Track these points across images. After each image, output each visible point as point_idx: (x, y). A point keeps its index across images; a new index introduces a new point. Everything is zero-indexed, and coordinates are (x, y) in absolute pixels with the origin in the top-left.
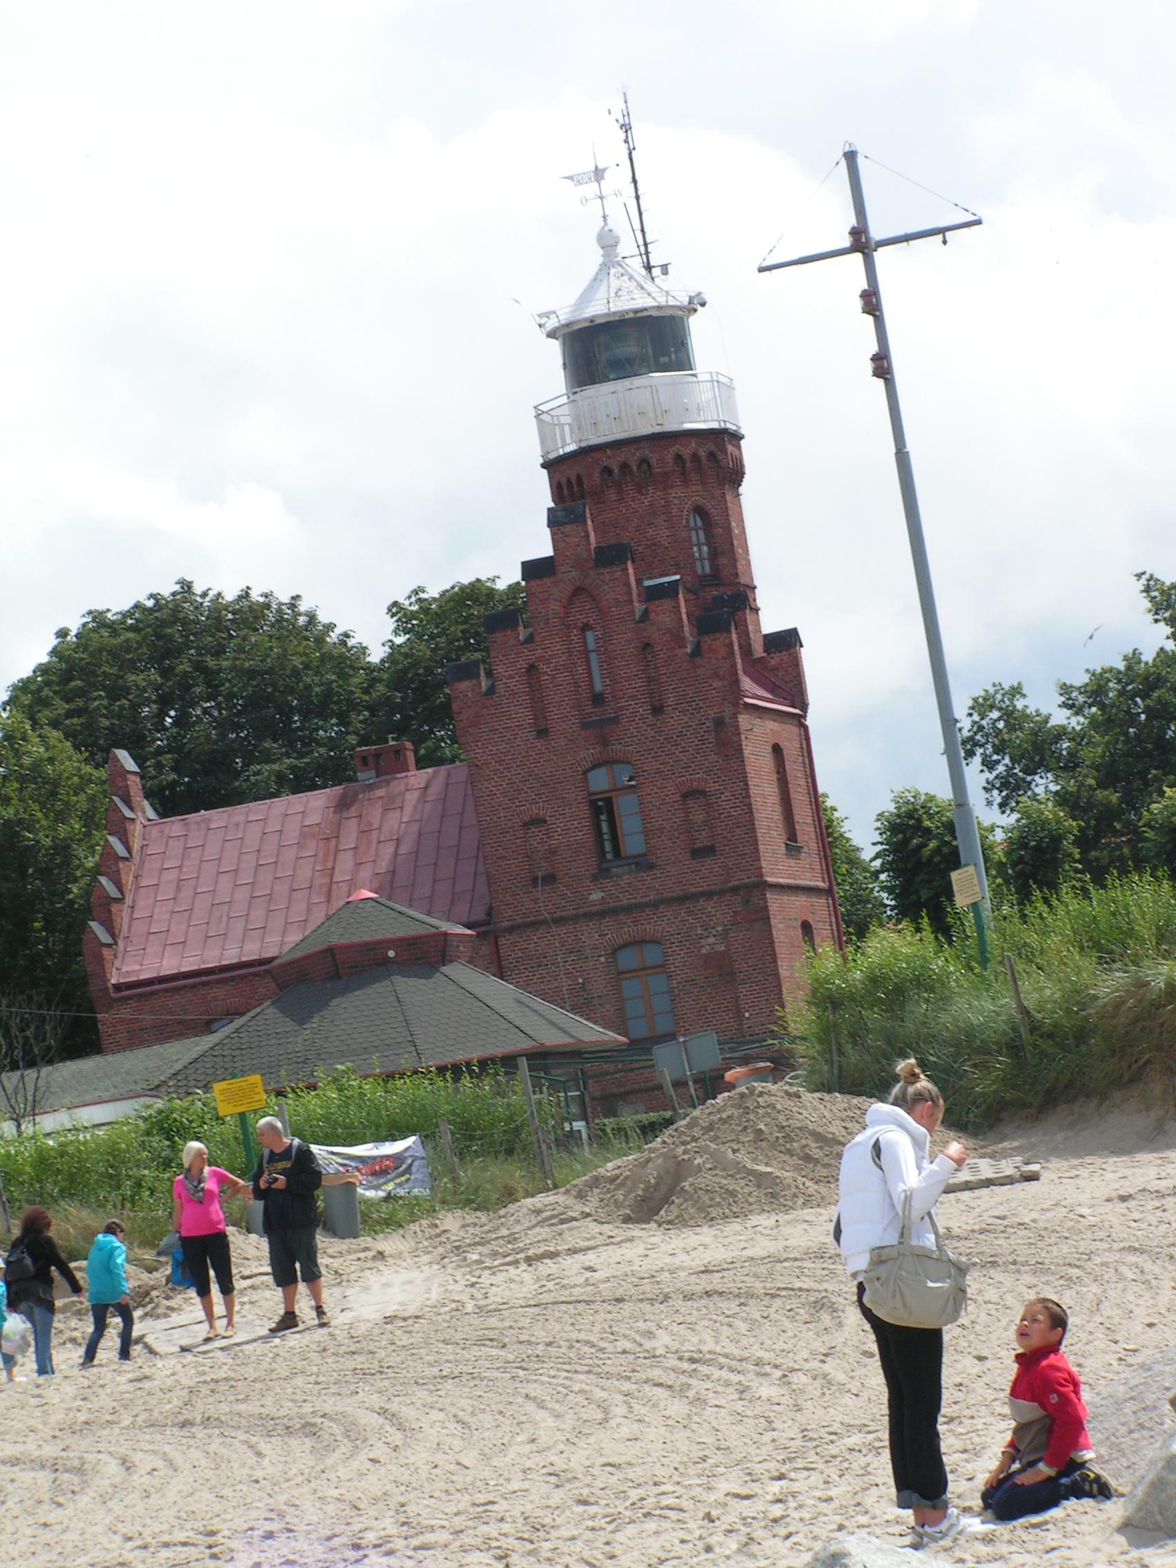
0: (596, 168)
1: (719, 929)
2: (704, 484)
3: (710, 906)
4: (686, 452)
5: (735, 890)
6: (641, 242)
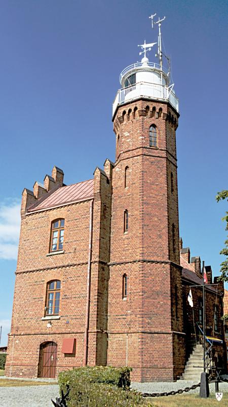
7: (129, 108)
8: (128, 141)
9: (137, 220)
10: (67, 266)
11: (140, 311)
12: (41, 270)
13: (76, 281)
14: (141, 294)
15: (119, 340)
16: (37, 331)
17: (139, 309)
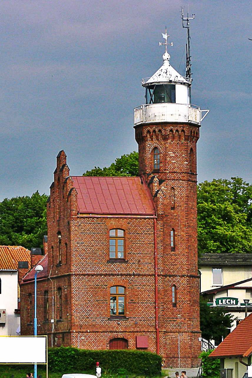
2: (158, 140)
7: (176, 128)
8: (174, 161)
9: (183, 240)
10: (133, 275)
11: (188, 316)
12: (103, 275)
13: (142, 290)
14: (189, 302)
15: (172, 338)
16: (104, 330)
17: (188, 314)
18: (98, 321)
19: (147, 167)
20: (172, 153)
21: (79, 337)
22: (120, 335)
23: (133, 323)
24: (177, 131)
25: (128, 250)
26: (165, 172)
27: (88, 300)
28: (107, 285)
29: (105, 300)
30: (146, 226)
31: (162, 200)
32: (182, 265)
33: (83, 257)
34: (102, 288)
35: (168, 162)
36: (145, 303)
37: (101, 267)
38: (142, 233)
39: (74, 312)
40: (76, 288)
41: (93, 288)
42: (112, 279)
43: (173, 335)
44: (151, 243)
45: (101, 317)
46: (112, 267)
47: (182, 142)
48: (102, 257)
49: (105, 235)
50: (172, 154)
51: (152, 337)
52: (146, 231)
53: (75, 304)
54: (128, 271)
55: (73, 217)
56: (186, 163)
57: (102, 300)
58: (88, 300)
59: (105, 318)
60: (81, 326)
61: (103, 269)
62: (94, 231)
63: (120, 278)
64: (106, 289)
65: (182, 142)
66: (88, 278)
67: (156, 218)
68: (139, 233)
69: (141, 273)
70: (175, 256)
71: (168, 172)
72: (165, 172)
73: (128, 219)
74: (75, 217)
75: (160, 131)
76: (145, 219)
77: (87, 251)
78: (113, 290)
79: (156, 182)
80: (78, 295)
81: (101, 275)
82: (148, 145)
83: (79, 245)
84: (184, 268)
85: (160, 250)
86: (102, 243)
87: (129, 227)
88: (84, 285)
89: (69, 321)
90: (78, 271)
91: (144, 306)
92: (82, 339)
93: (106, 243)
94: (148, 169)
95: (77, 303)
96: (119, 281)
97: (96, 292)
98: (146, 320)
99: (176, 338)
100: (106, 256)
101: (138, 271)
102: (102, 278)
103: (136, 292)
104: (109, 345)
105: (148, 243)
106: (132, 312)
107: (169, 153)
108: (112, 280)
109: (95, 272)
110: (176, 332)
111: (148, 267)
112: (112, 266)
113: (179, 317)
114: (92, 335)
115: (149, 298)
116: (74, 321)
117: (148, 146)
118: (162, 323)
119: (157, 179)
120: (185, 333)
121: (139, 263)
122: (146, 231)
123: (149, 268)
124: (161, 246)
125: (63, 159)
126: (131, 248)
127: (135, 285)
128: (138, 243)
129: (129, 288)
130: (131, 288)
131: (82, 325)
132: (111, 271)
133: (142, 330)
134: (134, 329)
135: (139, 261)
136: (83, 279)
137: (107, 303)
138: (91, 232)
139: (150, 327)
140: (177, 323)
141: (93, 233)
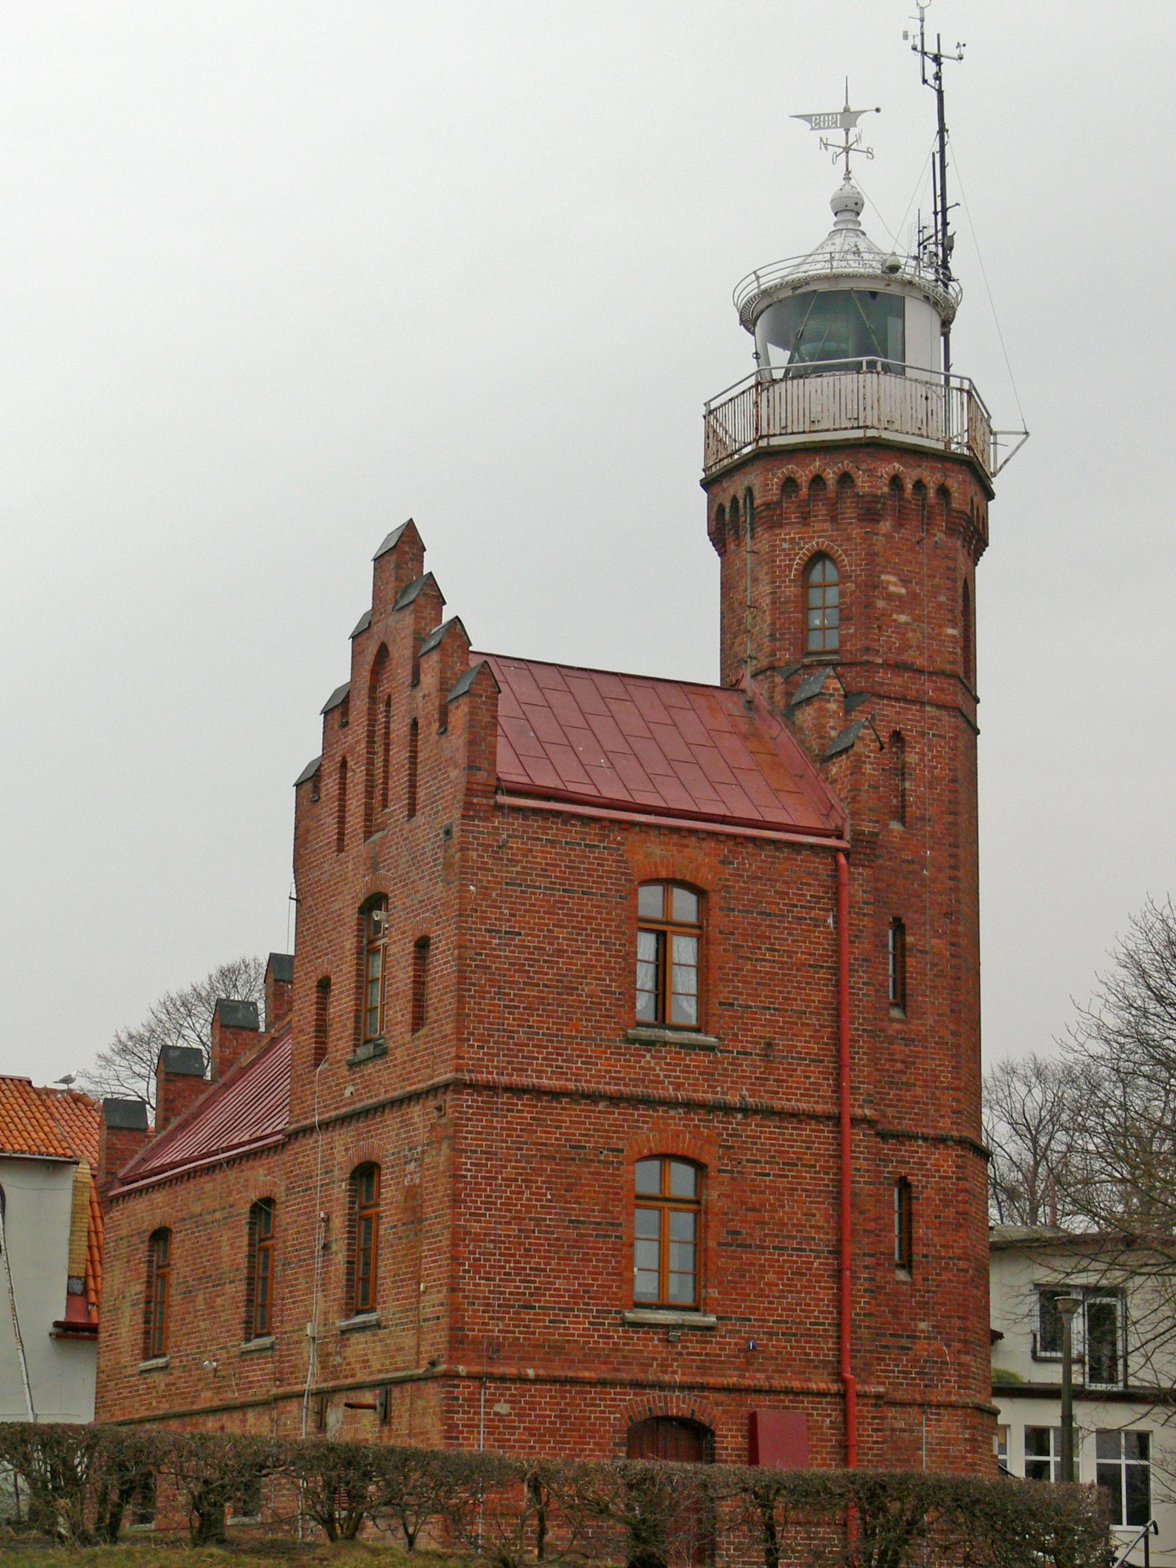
0: (847, 110)
1: (419, 1149)
2: (833, 519)
3: (415, 1111)
4: (803, 475)
5: (434, 1090)
6: (939, 208)
8: (903, 618)
11: (959, 1329)
13: (782, 1183)
15: (893, 1430)
18: (577, 1327)
19: (780, 640)
20: (893, 579)
21: (482, 1403)
22: (680, 1405)
23: (736, 1344)
24: (919, 485)
25: (721, 988)
26: (865, 658)
27: (530, 1219)
28: (621, 1151)
29: (612, 1224)
30: (802, 884)
31: (874, 769)
32: (937, 1088)
33: (512, 1000)
34: (599, 1161)
35: (878, 619)
36: (793, 1249)
37: (597, 1057)
38: (783, 916)
39: (465, 1271)
40: (476, 1152)
41: (555, 1158)
42: (647, 1122)
43: (897, 1419)
44: (822, 967)
45: (588, 1304)
46: (649, 1062)
47: (936, 539)
48: (603, 1012)
49: (617, 903)
50: (895, 584)
51: (823, 1422)
52: (802, 907)
53: (467, 1233)
54: (719, 1089)
55: (475, 800)
56: (950, 631)
57: (599, 1224)
58: (530, 1219)
59: (610, 1312)
60: (494, 1349)
61: (606, 1071)
62: (568, 879)
63: (680, 1119)
64: (618, 1169)
65: (936, 539)
66: (536, 1106)
67: (847, 853)
68: (770, 915)
69: (777, 1104)
70: (906, 1045)
71: (880, 661)
72: (867, 662)
73: (723, 838)
74: (485, 801)
75: (845, 479)
76: (796, 847)
77: (535, 972)
78: (646, 1178)
79: (831, 695)
80: (485, 1190)
81: (593, 1097)
82: (785, 546)
83: (497, 941)
84: (944, 1106)
85: (860, 1000)
86: (601, 943)
87: (726, 880)
88: (512, 1142)
89: (424, 1320)
90: (487, 1067)
91: (787, 1265)
92: (496, 1414)
93: (624, 945)
94: (780, 650)
95: (476, 1228)
96: (677, 1134)
97: (567, 1177)
98: (795, 1335)
99: (912, 1431)
100: (623, 1006)
101: (765, 1092)
102: (600, 1112)
103: (752, 1192)
104: (624, 1449)
105: (810, 966)
106: (735, 1288)
107: (883, 577)
108: (649, 1131)
109: (570, 1080)
110: (910, 1405)
111: (806, 1077)
112: (648, 1057)
113: (922, 1331)
114: (546, 1397)
115: (811, 1227)
116: (463, 1316)
117: (784, 550)
118: (866, 1351)
119: (839, 686)
120: (951, 1411)
121: (766, 1055)
122: (802, 907)
123: (812, 1080)
124: (864, 983)
125: (411, 560)
126: (733, 981)
127: (748, 1161)
128: (765, 960)
129: (720, 1171)
130: (732, 1172)
131: (499, 1344)
132: (643, 1081)
133: (777, 1383)
134: (739, 1376)
135: (769, 1045)
136: (509, 1110)
137: (619, 1237)
138: (555, 883)
139: (816, 1367)
140: (915, 1361)
141: (564, 891)
